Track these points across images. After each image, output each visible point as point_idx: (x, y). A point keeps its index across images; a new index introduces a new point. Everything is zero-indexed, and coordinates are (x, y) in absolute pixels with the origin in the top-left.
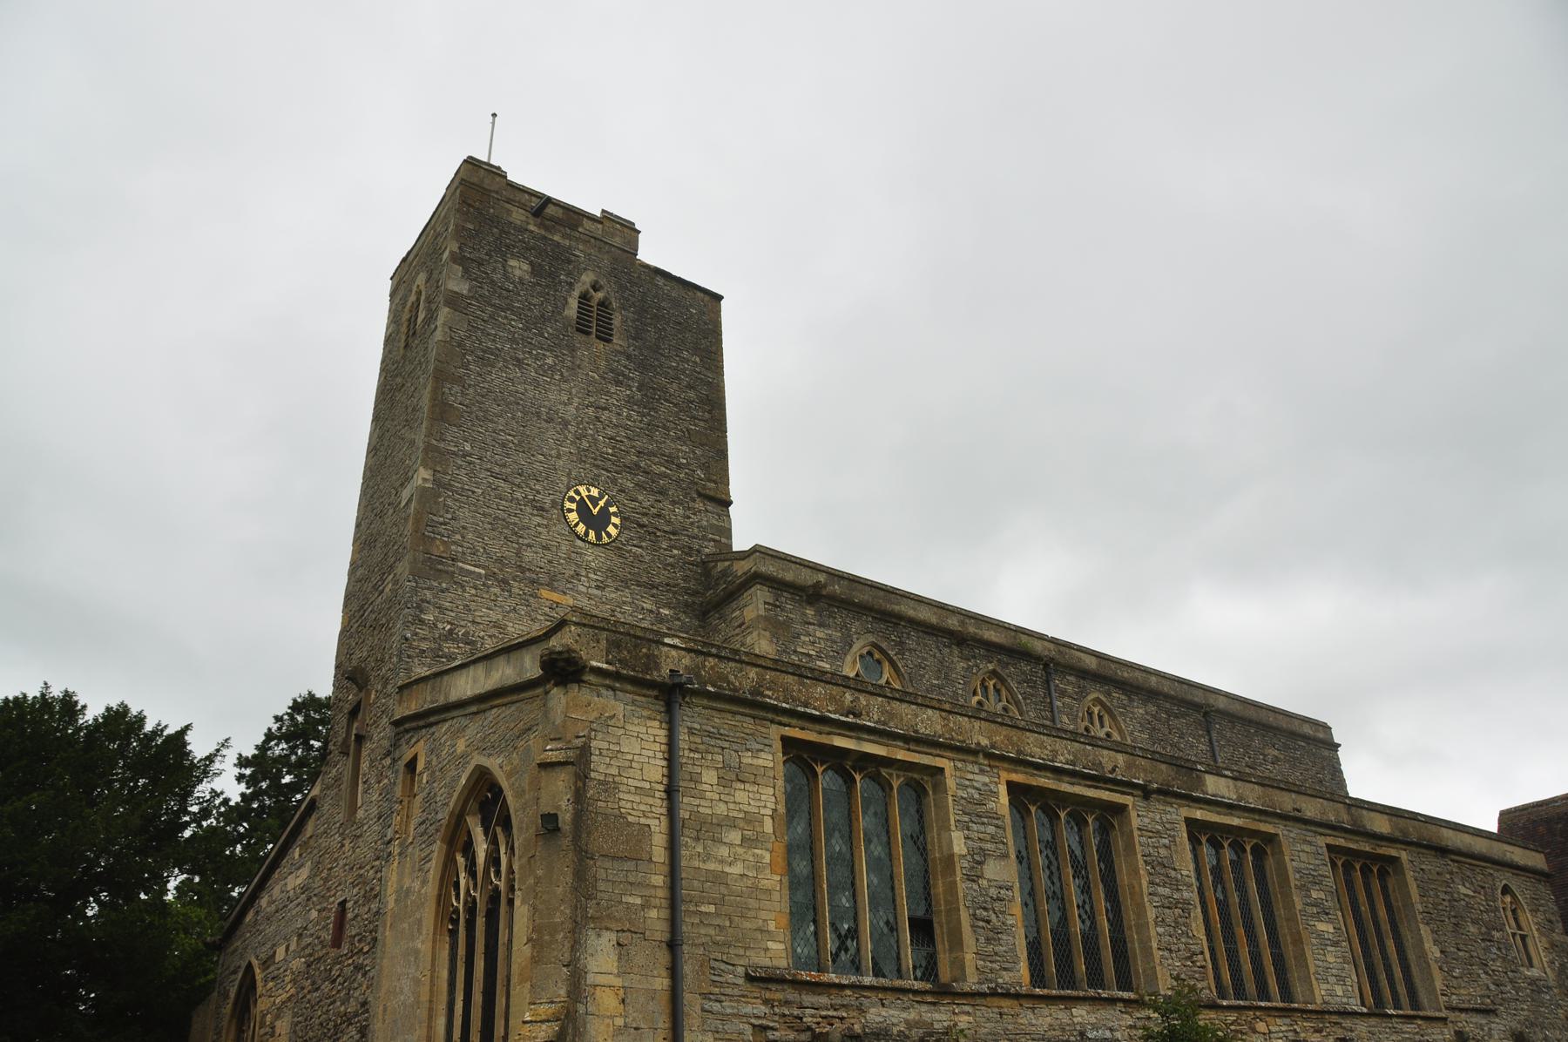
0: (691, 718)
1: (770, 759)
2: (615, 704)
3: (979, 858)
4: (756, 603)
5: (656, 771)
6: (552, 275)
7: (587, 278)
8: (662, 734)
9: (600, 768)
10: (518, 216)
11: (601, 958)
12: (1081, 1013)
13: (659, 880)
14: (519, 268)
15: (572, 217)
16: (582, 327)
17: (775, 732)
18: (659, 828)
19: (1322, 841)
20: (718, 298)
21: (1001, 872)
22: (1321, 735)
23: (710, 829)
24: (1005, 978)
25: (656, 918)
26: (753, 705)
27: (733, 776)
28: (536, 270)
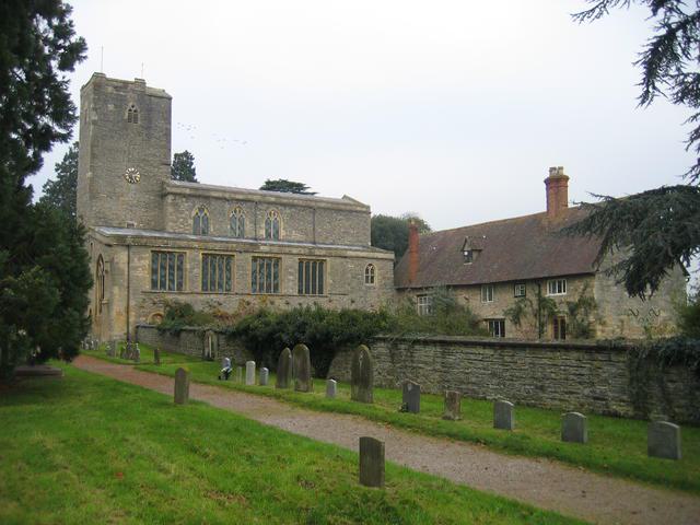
0: (133, 250)
1: (148, 255)
2: (119, 249)
3: (192, 269)
4: (170, 199)
5: (126, 259)
6: (121, 107)
7: (131, 104)
8: (126, 253)
9: (116, 260)
10: (110, 89)
11: (116, 290)
12: (212, 296)
13: (126, 277)
14: (111, 107)
15: (126, 84)
16: (129, 120)
17: (149, 250)
18: (126, 269)
19: (297, 258)
20: (170, 99)
21: (198, 271)
22: (364, 209)
23: (136, 268)
24: (196, 290)
25: (126, 284)
26: (145, 246)
27: (139, 260)
28: (116, 106)
